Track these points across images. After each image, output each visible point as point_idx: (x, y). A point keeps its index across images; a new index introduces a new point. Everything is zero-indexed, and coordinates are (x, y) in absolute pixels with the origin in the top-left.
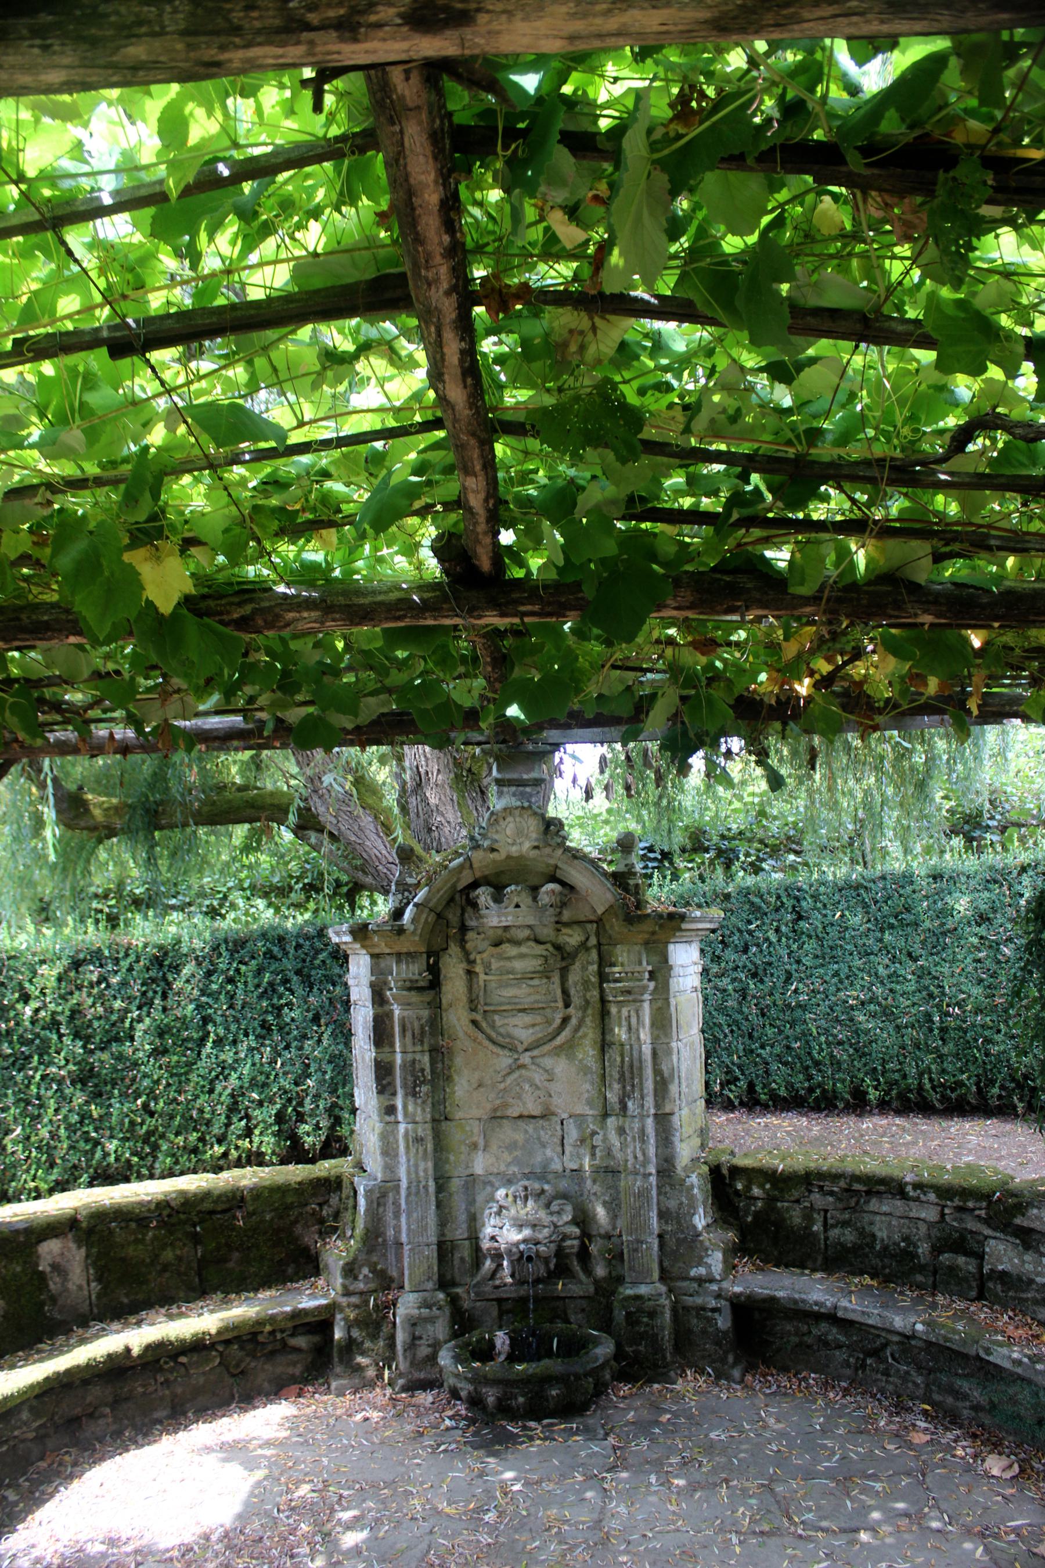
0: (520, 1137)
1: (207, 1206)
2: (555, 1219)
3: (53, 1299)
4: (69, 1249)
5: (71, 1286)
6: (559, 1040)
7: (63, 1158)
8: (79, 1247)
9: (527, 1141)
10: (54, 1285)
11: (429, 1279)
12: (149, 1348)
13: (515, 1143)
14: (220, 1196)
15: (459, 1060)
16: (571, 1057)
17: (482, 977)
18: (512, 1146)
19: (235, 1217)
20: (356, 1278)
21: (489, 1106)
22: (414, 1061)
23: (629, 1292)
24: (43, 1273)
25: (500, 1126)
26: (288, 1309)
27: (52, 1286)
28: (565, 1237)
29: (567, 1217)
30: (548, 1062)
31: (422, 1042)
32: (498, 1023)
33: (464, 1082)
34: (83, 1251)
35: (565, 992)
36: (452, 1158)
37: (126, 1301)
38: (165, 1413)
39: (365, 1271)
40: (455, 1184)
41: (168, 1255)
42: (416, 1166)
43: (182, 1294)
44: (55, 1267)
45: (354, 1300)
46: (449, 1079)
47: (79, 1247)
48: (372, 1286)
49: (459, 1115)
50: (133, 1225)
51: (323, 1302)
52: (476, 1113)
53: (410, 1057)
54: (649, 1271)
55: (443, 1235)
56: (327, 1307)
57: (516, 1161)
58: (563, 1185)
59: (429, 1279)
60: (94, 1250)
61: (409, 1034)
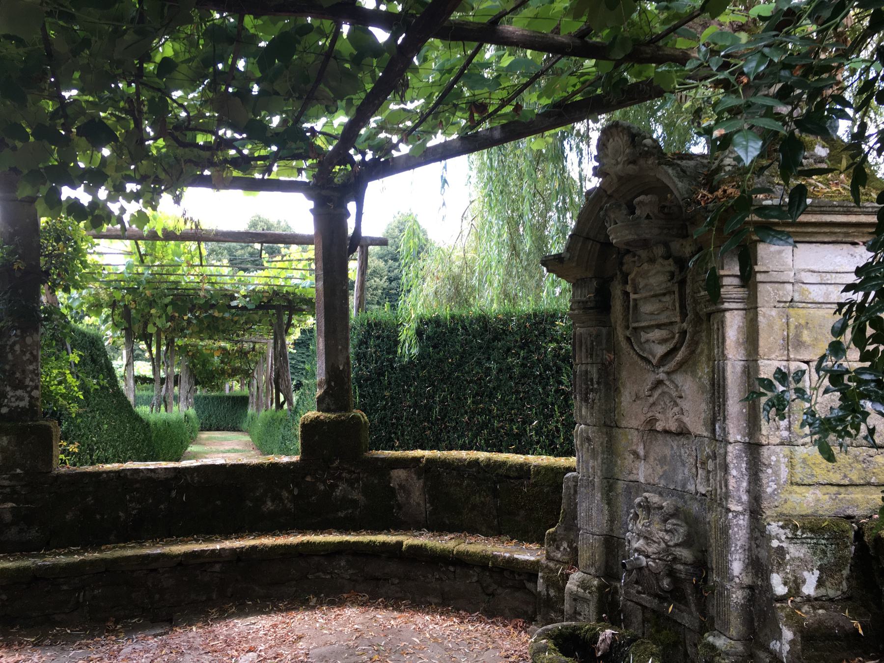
0: (667, 452)
1: (501, 471)
2: (667, 537)
3: (400, 507)
4: (412, 479)
5: (412, 501)
6: (679, 356)
7: (561, 445)
8: (419, 479)
9: (672, 456)
10: (401, 497)
11: (593, 565)
12: (411, 547)
13: (665, 457)
14: (511, 466)
15: (624, 374)
16: (694, 374)
17: (632, 296)
18: (662, 461)
19: (522, 484)
20: (558, 548)
21: (643, 418)
22: (586, 371)
23: (711, 639)
24: (393, 488)
25: (656, 440)
26: (507, 555)
27: (399, 498)
28: (675, 559)
29: (678, 539)
30: (679, 378)
31: (591, 357)
32: (643, 340)
33: (627, 393)
34: (421, 481)
35: (683, 307)
36: (619, 462)
37: (447, 522)
38: (436, 601)
39: (565, 545)
40: (621, 485)
41: (477, 499)
42: (587, 463)
43: (484, 530)
44: (401, 487)
45: (551, 565)
46: (617, 390)
47: (419, 479)
48: (566, 558)
49: (624, 424)
50: (455, 473)
51: (532, 559)
52: (634, 423)
53: (583, 368)
54: (727, 624)
55: (612, 530)
56: (532, 563)
57: (664, 476)
58: (695, 507)
59: (593, 565)
60: (429, 483)
61: (584, 350)
